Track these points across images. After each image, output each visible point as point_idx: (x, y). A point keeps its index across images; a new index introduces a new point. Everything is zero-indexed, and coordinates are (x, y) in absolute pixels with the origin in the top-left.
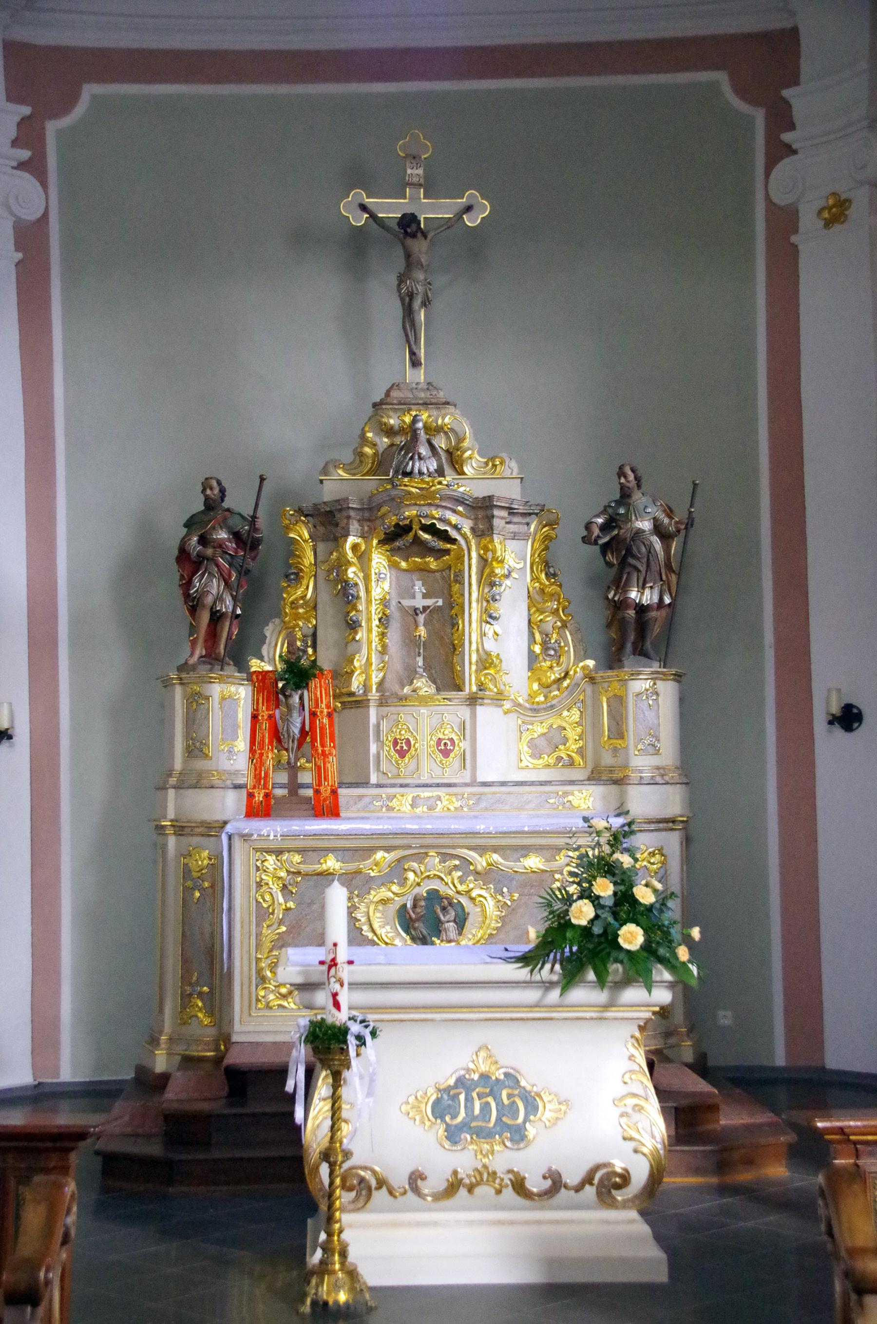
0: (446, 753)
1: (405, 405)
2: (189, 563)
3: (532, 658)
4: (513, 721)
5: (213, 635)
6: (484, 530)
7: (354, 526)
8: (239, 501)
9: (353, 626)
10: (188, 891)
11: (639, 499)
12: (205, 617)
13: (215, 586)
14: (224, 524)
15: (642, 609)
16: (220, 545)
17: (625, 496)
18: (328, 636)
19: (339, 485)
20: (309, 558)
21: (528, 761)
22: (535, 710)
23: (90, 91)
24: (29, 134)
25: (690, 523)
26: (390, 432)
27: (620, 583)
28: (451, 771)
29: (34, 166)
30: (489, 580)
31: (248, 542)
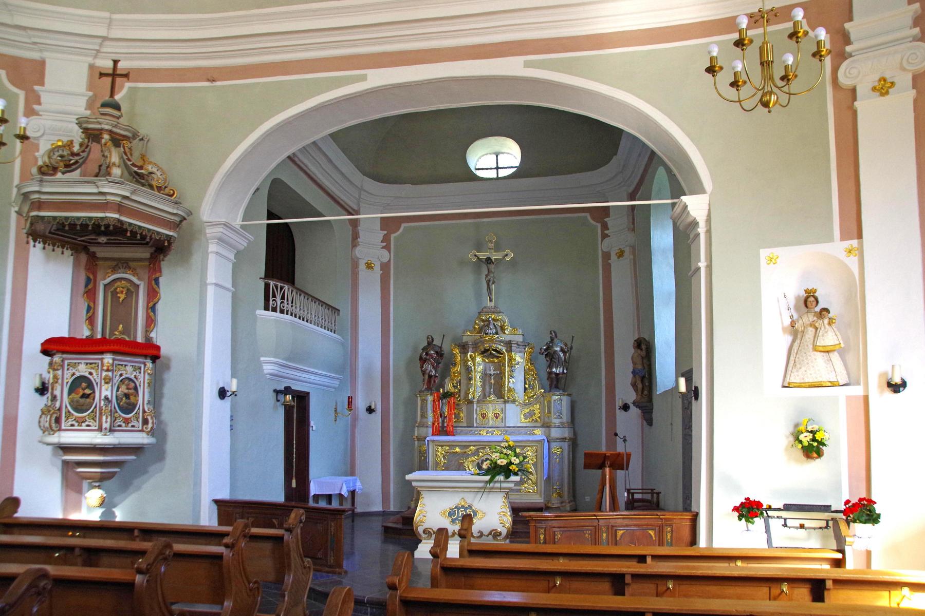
0: (497, 418)
1: (487, 313)
2: (423, 361)
3: (525, 389)
4: (519, 408)
5: (429, 382)
6: (509, 351)
7: (471, 349)
8: (437, 342)
9: (470, 379)
10: (420, 457)
11: (556, 341)
12: (427, 377)
13: (430, 367)
14: (433, 349)
15: (557, 374)
16: (431, 355)
17: (552, 340)
18: (464, 382)
19: (468, 337)
20: (459, 358)
21: (523, 420)
22: (526, 404)
23: (403, 225)
24: (386, 239)
25: (571, 348)
26: (483, 321)
27: (550, 367)
28: (498, 423)
29: (387, 248)
30: (511, 367)
31: (440, 354)
